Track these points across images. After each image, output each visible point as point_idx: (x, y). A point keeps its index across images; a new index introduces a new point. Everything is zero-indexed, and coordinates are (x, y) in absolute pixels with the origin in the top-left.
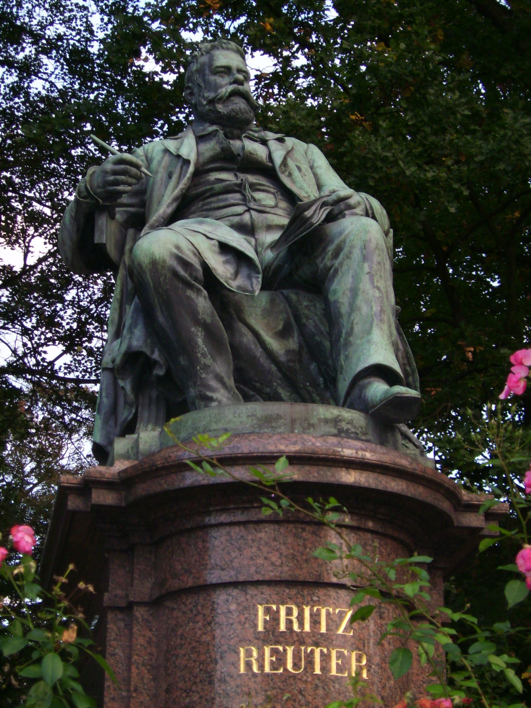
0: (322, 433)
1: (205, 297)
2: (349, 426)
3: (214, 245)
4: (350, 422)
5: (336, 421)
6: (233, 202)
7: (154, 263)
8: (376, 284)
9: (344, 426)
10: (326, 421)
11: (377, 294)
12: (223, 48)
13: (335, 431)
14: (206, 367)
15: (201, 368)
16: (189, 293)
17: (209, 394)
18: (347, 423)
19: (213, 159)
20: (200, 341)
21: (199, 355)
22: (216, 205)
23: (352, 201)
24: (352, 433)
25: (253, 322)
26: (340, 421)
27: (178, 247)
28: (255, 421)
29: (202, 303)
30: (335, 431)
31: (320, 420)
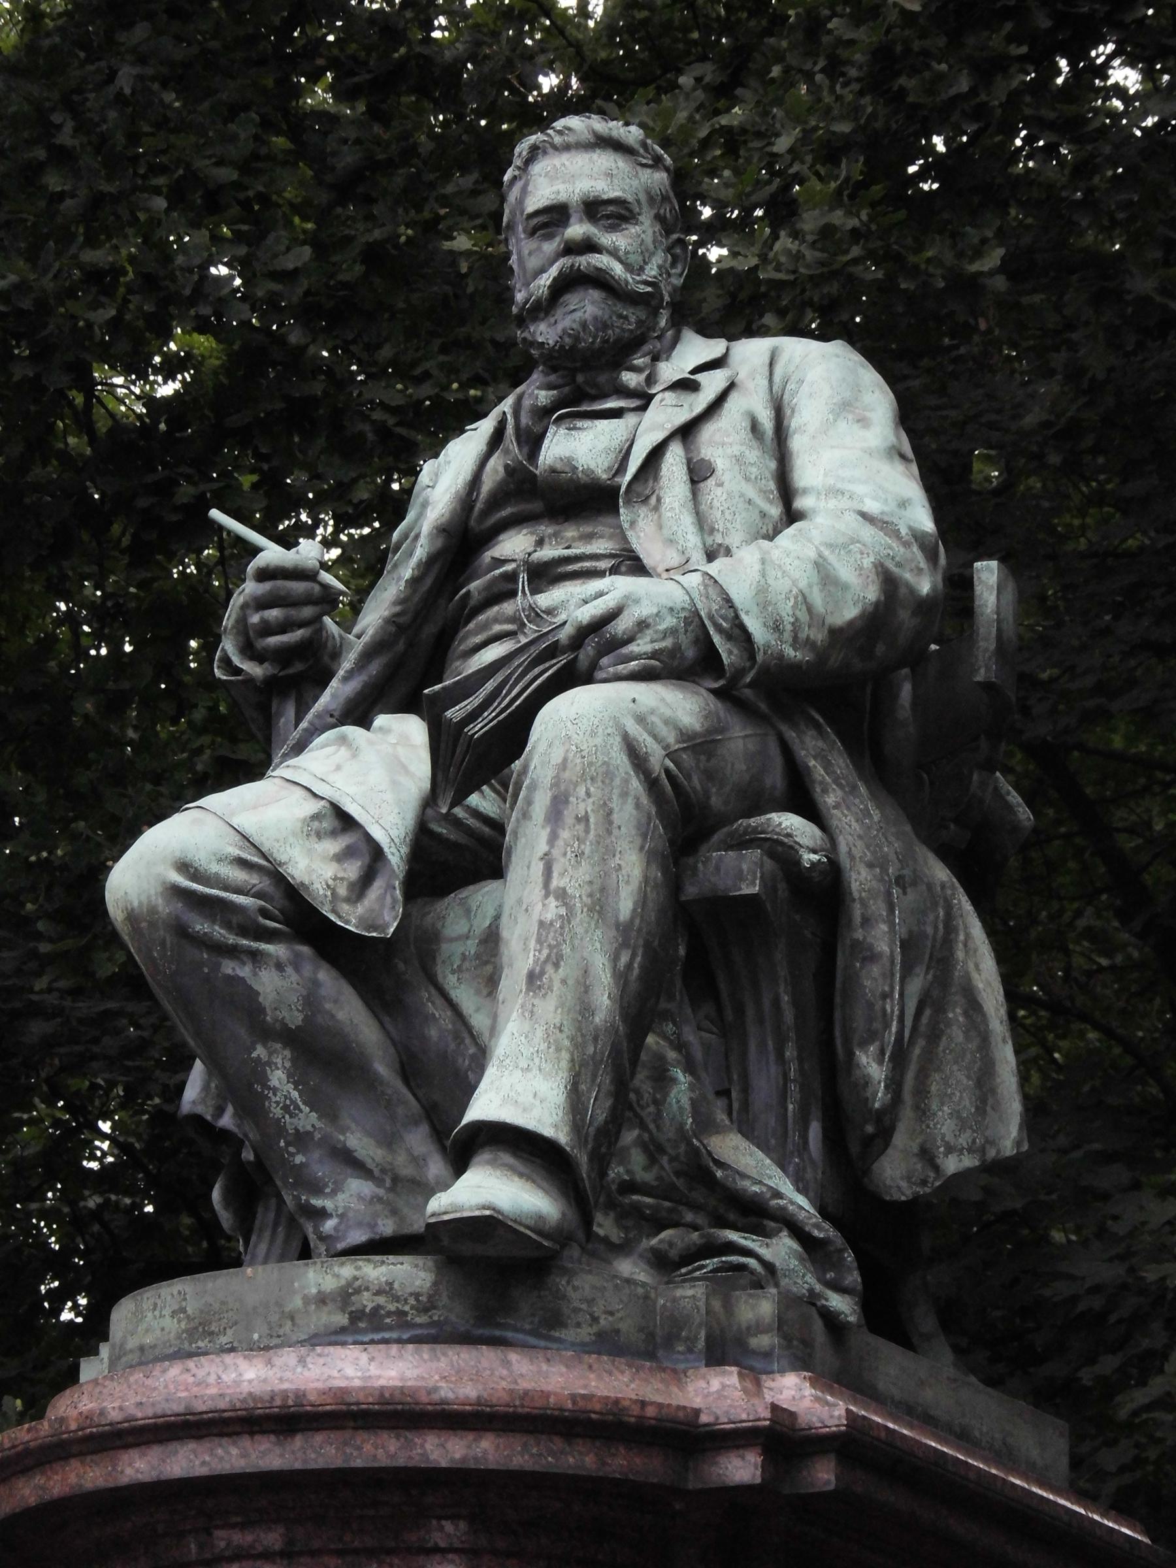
0: (312, 1329)
1: (280, 967)
2: (381, 1300)
3: (316, 817)
4: (386, 1290)
5: (345, 1295)
6: (497, 628)
7: (132, 917)
8: (555, 883)
9: (367, 1301)
10: (322, 1299)
11: (553, 910)
12: (555, 148)
13: (342, 1320)
14: (301, 1139)
15: (288, 1144)
16: (229, 967)
17: (317, 1202)
18: (378, 1293)
19: (498, 499)
20: (278, 1077)
21: (277, 1112)
22: (478, 639)
23: (622, 625)
24: (389, 1314)
25: (450, 981)
26: (358, 1291)
27: (184, 867)
28: (183, 1325)
29: (280, 979)
30: (342, 1320)
31: (307, 1300)
